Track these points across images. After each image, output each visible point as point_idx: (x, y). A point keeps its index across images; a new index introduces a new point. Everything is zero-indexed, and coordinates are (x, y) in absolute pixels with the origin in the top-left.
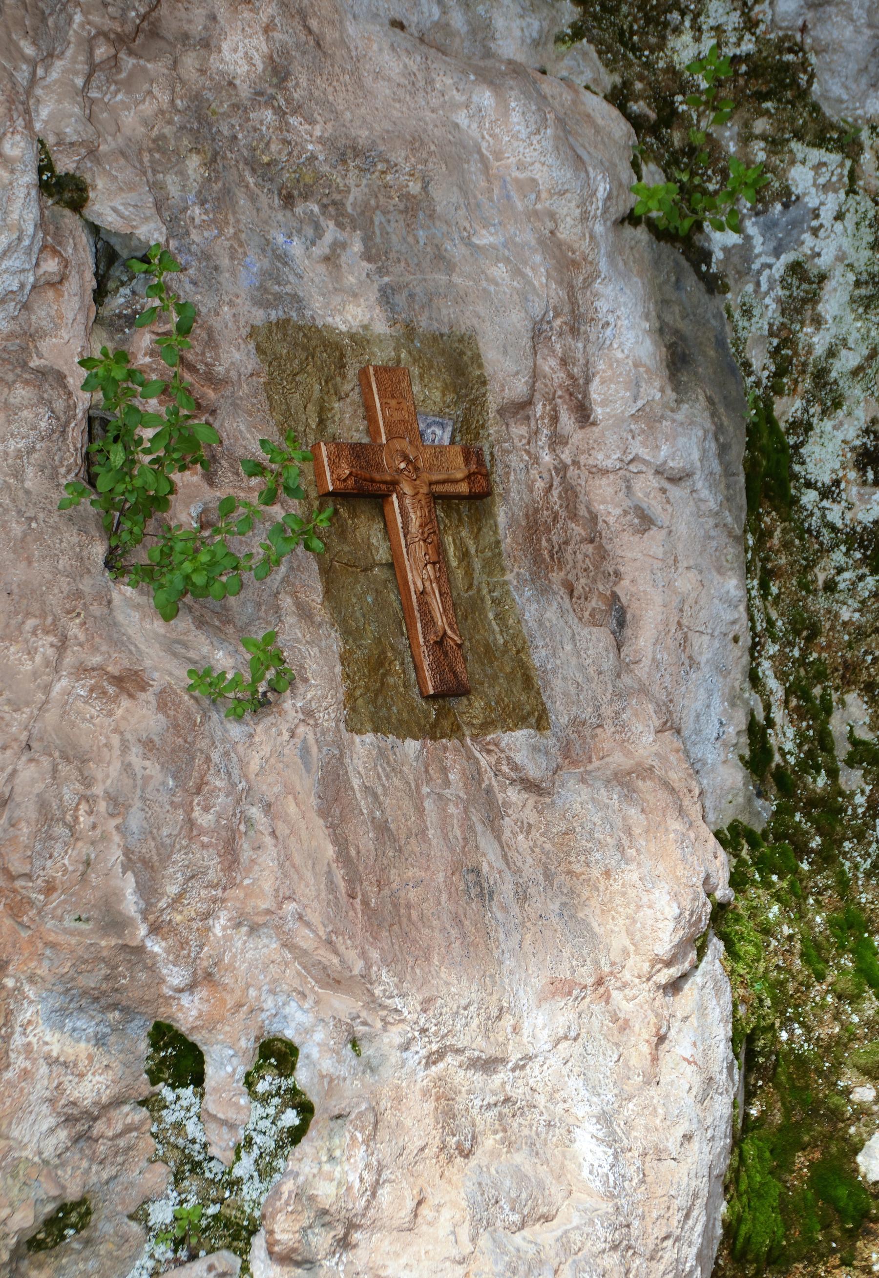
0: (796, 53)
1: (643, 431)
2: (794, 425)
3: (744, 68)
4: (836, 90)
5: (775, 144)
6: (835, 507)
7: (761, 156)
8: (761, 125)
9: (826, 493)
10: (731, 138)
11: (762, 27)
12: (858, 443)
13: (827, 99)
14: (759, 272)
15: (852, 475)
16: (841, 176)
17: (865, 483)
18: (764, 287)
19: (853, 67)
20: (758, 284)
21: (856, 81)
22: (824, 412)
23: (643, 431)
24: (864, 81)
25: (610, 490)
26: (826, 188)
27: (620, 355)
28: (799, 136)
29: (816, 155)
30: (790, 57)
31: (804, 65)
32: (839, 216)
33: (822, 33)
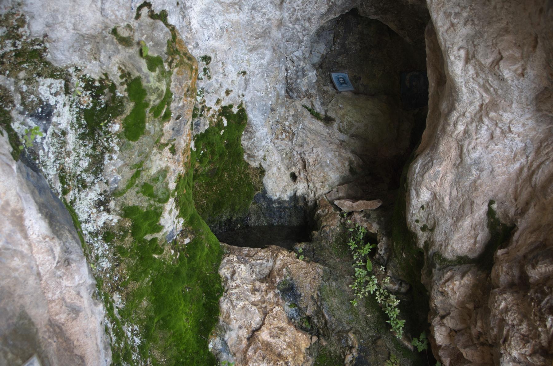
0: (40, 45)
1: (65, 274)
2: (72, 202)
3: (14, 54)
4: (59, 56)
5: (29, 81)
6: (90, 224)
7: (25, 88)
8: (22, 75)
9: (86, 223)
10: (11, 85)
11: (24, 37)
12: (96, 199)
13: (55, 60)
14: (42, 144)
15: (94, 210)
16: (61, 88)
17: (100, 212)
18: (46, 149)
19: (67, 46)
20: (44, 150)
21: (68, 51)
22: (79, 191)
23: (65, 274)
24: (71, 50)
25: (58, 307)
26: (56, 94)
27: (34, 236)
28: (39, 75)
29: (49, 81)
30: (38, 47)
31: (45, 49)
32: (65, 105)
33: (53, 36)
